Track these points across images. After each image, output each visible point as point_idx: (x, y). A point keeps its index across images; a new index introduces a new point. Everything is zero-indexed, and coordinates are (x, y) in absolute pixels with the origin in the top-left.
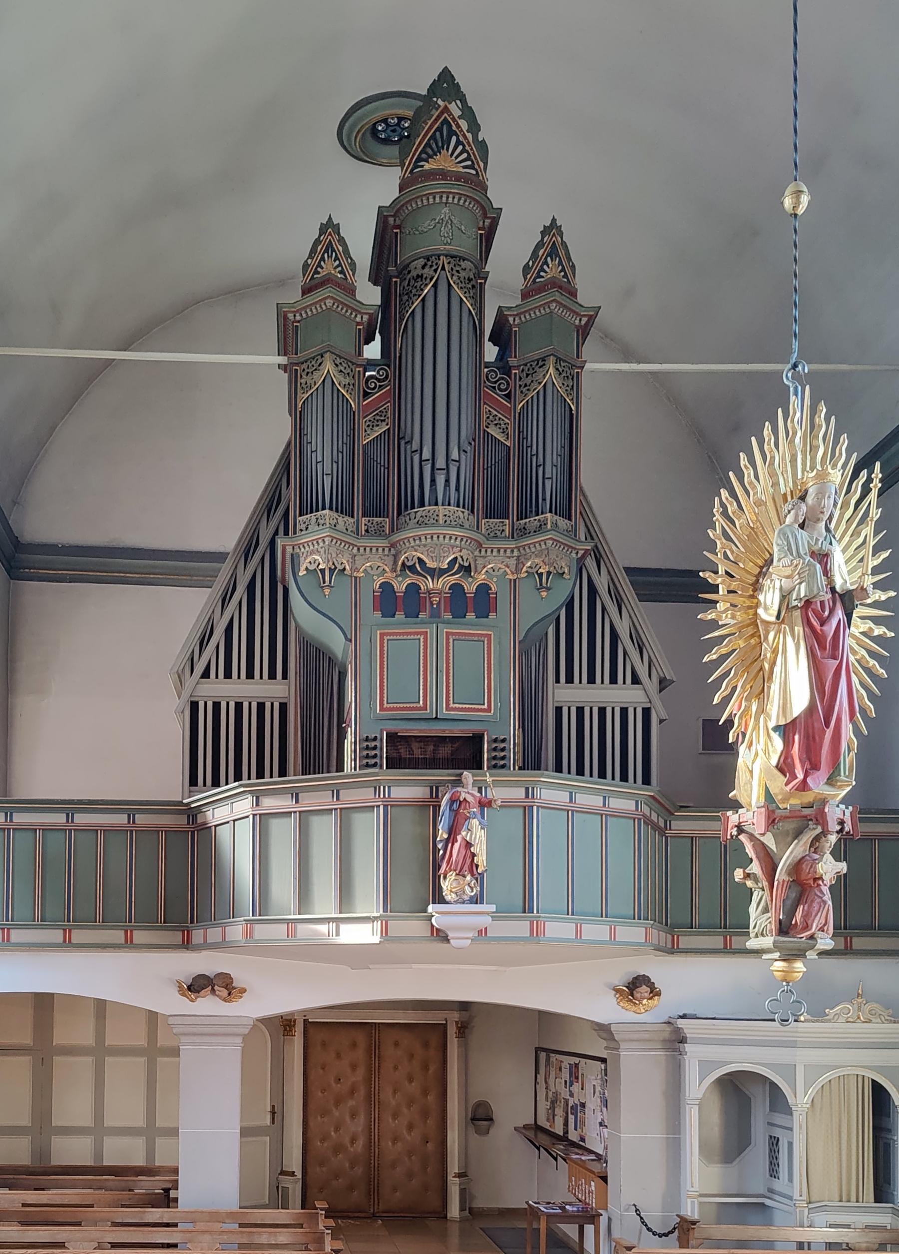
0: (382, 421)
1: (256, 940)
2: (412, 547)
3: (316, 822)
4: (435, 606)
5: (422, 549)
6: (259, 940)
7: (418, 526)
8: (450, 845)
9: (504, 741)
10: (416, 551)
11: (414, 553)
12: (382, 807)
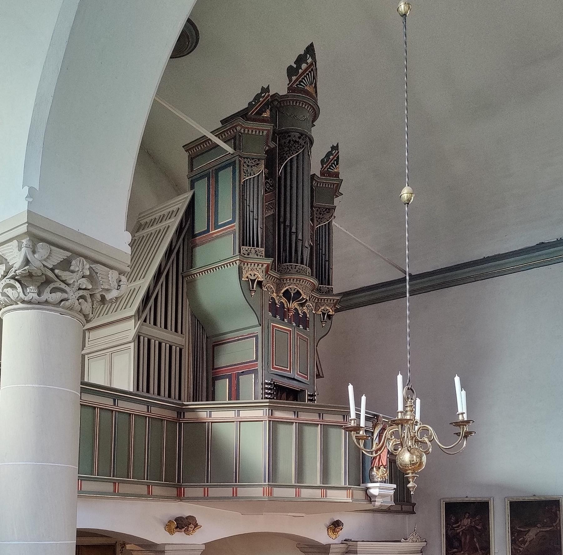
0: (272, 208)
4: (290, 317)
5: (299, 286)
7: (297, 273)
11: (296, 287)
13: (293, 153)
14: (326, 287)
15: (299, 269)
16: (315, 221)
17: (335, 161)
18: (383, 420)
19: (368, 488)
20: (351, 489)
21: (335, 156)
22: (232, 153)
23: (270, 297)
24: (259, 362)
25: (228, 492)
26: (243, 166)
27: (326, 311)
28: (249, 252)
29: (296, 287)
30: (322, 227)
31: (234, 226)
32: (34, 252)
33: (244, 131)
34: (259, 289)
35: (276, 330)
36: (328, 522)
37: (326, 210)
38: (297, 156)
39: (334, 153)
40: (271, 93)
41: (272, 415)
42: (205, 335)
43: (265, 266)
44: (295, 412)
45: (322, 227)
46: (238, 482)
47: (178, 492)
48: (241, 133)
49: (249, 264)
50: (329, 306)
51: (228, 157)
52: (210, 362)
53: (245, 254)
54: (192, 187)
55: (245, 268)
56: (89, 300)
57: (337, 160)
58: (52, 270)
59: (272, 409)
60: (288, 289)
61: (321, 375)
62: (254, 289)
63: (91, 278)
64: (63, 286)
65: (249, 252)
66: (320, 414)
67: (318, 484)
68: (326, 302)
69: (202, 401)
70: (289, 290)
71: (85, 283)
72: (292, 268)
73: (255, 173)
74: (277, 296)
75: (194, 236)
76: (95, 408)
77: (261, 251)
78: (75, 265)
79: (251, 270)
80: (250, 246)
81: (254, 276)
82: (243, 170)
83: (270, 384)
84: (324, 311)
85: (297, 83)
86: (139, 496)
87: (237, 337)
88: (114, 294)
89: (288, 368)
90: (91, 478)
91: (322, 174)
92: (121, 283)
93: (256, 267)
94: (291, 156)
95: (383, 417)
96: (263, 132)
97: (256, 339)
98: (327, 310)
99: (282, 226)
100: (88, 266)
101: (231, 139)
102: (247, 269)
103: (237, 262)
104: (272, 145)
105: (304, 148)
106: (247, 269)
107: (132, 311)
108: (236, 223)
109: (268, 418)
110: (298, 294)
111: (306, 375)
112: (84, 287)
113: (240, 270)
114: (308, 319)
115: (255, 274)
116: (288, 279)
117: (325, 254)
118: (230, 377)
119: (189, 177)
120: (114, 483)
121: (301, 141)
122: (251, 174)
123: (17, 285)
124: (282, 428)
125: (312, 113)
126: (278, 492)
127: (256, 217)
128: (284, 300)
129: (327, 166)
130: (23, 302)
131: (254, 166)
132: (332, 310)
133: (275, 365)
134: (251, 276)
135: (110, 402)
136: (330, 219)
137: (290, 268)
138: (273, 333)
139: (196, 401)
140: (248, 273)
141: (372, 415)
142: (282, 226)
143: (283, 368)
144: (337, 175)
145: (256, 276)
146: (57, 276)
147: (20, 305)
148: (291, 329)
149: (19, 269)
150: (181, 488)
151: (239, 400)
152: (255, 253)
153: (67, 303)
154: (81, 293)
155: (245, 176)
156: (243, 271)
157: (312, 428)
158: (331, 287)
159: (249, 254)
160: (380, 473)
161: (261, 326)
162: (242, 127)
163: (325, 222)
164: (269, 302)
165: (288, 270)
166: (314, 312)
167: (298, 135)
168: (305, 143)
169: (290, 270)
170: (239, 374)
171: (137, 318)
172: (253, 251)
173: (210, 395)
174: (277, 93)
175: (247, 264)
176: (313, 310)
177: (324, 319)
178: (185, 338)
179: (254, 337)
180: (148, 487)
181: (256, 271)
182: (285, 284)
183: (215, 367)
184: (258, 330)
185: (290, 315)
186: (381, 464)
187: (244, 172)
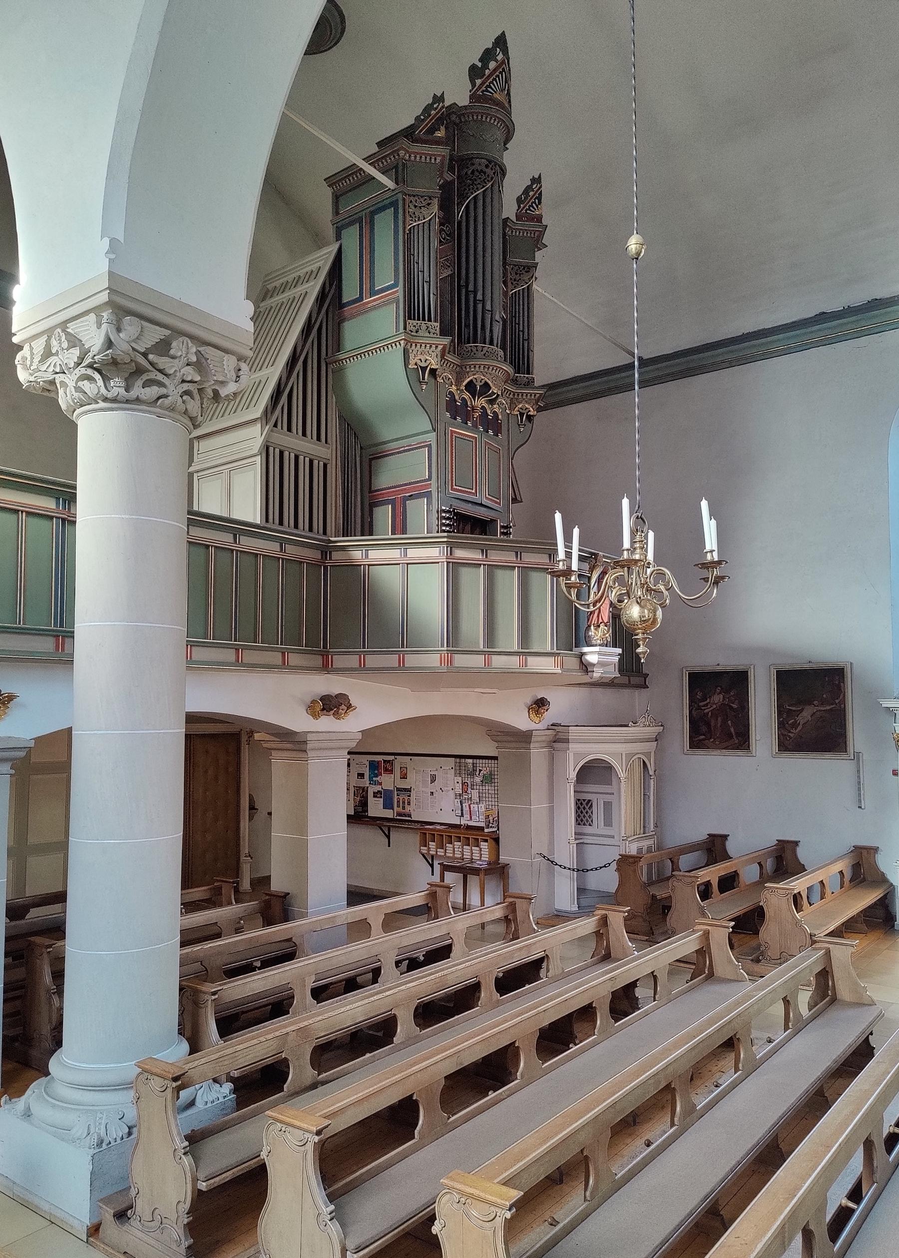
0: (449, 267)
2: (481, 372)
7: (484, 357)
11: (483, 378)
13: (477, 189)
16: (509, 284)
18: (604, 560)
19: (582, 654)
25: (392, 660)
26: (409, 206)
29: (483, 378)
31: (397, 292)
32: (119, 330)
33: (410, 156)
34: (433, 380)
36: (529, 700)
37: (524, 269)
40: (447, 104)
43: (440, 347)
48: (406, 161)
50: (529, 404)
51: (389, 194)
53: (412, 332)
54: (338, 237)
56: (197, 397)
57: (539, 198)
58: (145, 355)
59: (452, 546)
60: (471, 381)
61: (519, 499)
62: (426, 380)
63: (199, 365)
64: (160, 377)
66: (517, 553)
67: (516, 649)
68: (524, 397)
71: (191, 373)
72: (477, 350)
74: (457, 389)
75: (342, 306)
76: (207, 547)
78: (177, 347)
80: (419, 319)
81: (425, 362)
82: (409, 212)
83: (448, 512)
87: (402, 448)
88: (231, 388)
90: (204, 642)
92: (241, 373)
94: (475, 192)
96: (435, 159)
99: (464, 291)
100: (194, 350)
103: (402, 342)
105: (492, 182)
108: (400, 288)
109: (447, 558)
110: (486, 386)
112: (189, 379)
113: (406, 353)
116: (472, 366)
118: (393, 503)
120: (236, 649)
121: (488, 171)
122: (419, 218)
123: (97, 376)
124: (465, 572)
126: (460, 660)
127: (426, 278)
128: (467, 395)
129: (526, 206)
130: (106, 399)
131: (424, 206)
132: (533, 409)
135: (228, 538)
137: (474, 350)
142: (464, 291)
143: (467, 490)
144: (539, 219)
146: (152, 364)
147: (102, 405)
149: (98, 354)
150: (327, 656)
151: (406, 534)
153: (167, 402)
154: (186, 387)
155: (412, 220)
156: (410, 355)
157: (508, 572)
161: (435, 431)
163: (522, 286)
165: (472, 354)
166: (508, 412)
168: (494, 173)
169: (475, 354)
171: (264, 422)
172: (424, 327)
175: (416, 345)
177: (522, 422)
180: (283, 653)
182: (468, 372)
183: (373, 489)
184: (431, 437)
186: (600, 620)
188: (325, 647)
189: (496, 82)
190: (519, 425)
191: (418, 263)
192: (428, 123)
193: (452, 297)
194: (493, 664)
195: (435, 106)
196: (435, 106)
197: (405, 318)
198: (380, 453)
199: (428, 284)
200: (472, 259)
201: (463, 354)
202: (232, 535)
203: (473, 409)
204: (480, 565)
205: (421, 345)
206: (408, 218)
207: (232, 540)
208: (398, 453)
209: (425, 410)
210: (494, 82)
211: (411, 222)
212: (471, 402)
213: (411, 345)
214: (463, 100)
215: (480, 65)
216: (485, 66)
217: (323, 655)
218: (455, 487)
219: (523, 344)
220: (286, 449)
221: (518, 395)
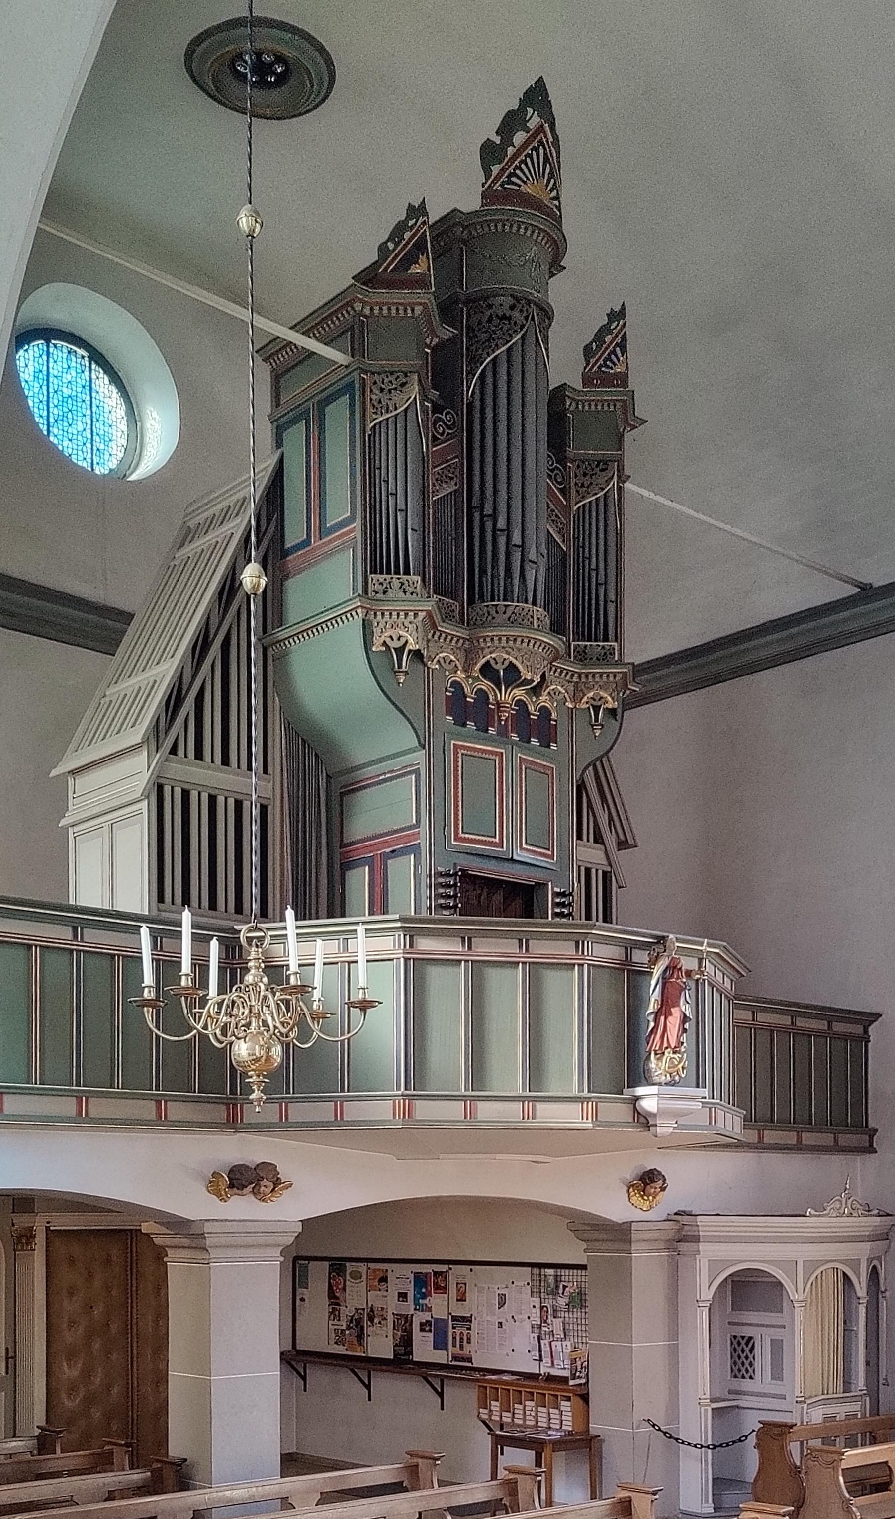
0: (451, 479)
1: (417, 1121)
3: (553, 980)
4: (503, 723)
6: (421, 1121)
8: (662, 1018)
9: (571, 894)
10: (508, 653)
11: (506, 656)
12: (402, 960)
13: (497, 345)
14: (599, 646)
15: (513, 613)
17: (618, 346)
19: (637, 1099)
20: (592, 1100)
21: (617, 336)
22: (345, 363)
23: (450, 681)
24: (424, 829)
25: (324, 1111)
26: (371, 391)
27: (599, 700)
28: (387, 588)
29: (506, 656)
30: (597, 505)
31: (351, 531)
33: (372, 309)
35: (462, 754)
37: (597, 466)
38: (509, 350)
39: (613, 329)
40: (433, 218)
41: (411, 946)
42: (324, 771)
43: (422, 615)
44: (463, 939)
45: (597, 505)
46: (346, 1090)
47: (228, 1115)
48: (366, 316)
49: (387, 613)
50: (605, 691)
52: (336, 831)
53: (377, 593)
54: (279, 443)
55: (378, 623)
57: (623, 346)
60: (488, 662)
61: (631, 841)
62: (404, 669)
65: (387, 588)
66: (520, 941)
67: (520, 1092)
69: (318, 918)
70: (492, 662)
72: (497, 612)
73: (397, 405)
74: (468, 677)
75: (285, 553)
76: (29, 947)
77: (413, 583)
79: (392, 627)
80: (389, 572)
81: (399, 639)
82: (371, 399)
83: (447, 875)
84: (595, 700)
85: (504, 179)
86: (46, 1122)
87: (381, 775)
89: (495, 838)
90: (29, 1088)
91: (587, 380)
93: (403, 620)
94: (493, 352)
95: (678, 940)
96: (413, 310)
97: (415, 777)
98: (601, 698)
99: (477, 515)
101: (346, 331)
102: (381, 626)
103: (359, 611)
104: (447, 332)
105: (522, 332)
106: (381, 626)
107: (136, 735)
108: (357, 524)
109: (404, 953)
110: (512, 667)
111: (548, 850)
113: (367, 627)
114: (555, 723)
115: (400, 636)
116: (488, 639)
117: (597, 569)
118: (370, 862)
119: (273, 419)
120: (156, 1101)
121: (516, 314)
122: (388, 408)
124: (434, 973)
125: (546, 244)
126: (424, 1110)
127: (401, 505)
128: (485, 685)
129: (597, 361)
131: (395, 389)
132: (613, 699)
133: (463, 832)
134: (392, 639)
135: (65, 933)
136: (608, 485)
137: (493, 612)
138: (456, 761)
139: (305, 919)
140: (386, 634)
141: (655, 939)
142: (477, 515)
144: (623, 379)
145: (403, 641)
148: (503, 751)
150: (235, 1106)
151: (387, 913)
152: (400, 588)
155: (376, 413)
156: (375, 630)
157: (507, 972)
158: (611, 645)
159: (387, 591)
160: (664, 1064)
161: (424, 747)
162: (365, 303)
163: (596, 494)
164: (447, 694)
165: (490, 618)
166: (571, 706)
167: (510, 301)
168: (526, 318)
169: (493, 618)
170: (386, 857)
171: (153, 747)
172: (396, 583)
173: (378, 903)
174: (455, 210)
175: (383, 614)
176: (566, 701)
177: (596, 720)
178: (272, 782)
179: (412, 774)
180: (158, 1103)
181: (402, 627)
182: (483, 649)
183: (345, 841)
185: (504, 718)
186: (665, 1045)
187: (374, 406)
188: (233, 1091)
189: (532, 160)
190: (592, 726)
191: (387, 482)
192: (397, 252)
193: (458, 527)
194: (479, 1116)
195: (411, 223)
196: (411, 223)
197: (366, 571)
198: (353, 784)
199: (403, 514)
200: (489, 459)
201: (476, 620)
202: (70, 928)
203: (499, 707)
204: (460, 961)
205: (391, 614)
206: (370, 410)
207: (70, 936)
208: (385, 781)
209: (405, 716)
210: (523, 166)
211: (374, 416)
212: (496, 695)
213: (375, 614)
214: (471, 202)
215: (497, 140)
216: (507, 141)
217: (228, 1105)
218: (463, 835)
219: (597, 590)
220: (191, 787)
221: (587, 676)
